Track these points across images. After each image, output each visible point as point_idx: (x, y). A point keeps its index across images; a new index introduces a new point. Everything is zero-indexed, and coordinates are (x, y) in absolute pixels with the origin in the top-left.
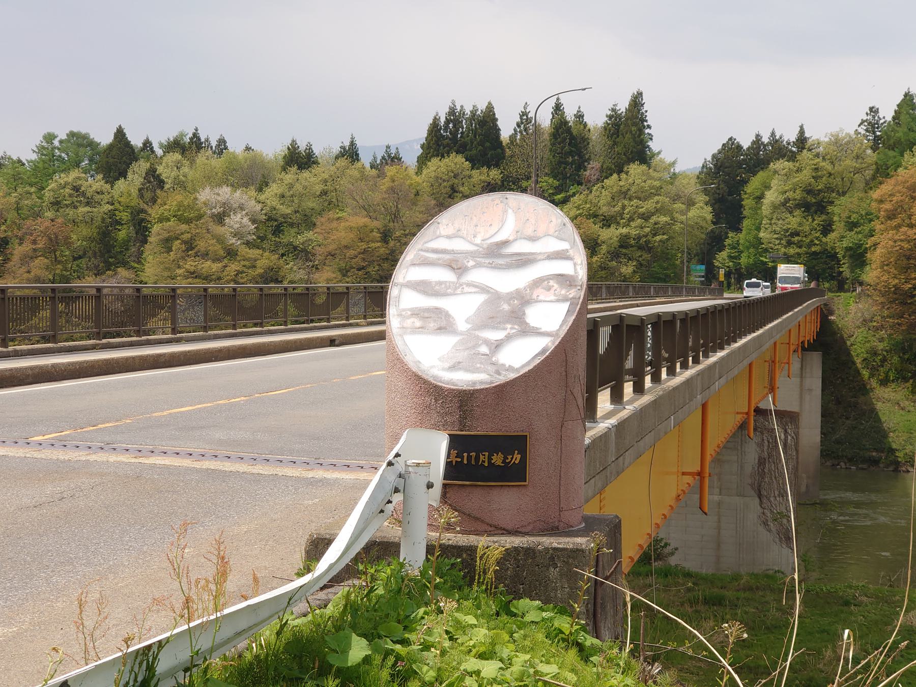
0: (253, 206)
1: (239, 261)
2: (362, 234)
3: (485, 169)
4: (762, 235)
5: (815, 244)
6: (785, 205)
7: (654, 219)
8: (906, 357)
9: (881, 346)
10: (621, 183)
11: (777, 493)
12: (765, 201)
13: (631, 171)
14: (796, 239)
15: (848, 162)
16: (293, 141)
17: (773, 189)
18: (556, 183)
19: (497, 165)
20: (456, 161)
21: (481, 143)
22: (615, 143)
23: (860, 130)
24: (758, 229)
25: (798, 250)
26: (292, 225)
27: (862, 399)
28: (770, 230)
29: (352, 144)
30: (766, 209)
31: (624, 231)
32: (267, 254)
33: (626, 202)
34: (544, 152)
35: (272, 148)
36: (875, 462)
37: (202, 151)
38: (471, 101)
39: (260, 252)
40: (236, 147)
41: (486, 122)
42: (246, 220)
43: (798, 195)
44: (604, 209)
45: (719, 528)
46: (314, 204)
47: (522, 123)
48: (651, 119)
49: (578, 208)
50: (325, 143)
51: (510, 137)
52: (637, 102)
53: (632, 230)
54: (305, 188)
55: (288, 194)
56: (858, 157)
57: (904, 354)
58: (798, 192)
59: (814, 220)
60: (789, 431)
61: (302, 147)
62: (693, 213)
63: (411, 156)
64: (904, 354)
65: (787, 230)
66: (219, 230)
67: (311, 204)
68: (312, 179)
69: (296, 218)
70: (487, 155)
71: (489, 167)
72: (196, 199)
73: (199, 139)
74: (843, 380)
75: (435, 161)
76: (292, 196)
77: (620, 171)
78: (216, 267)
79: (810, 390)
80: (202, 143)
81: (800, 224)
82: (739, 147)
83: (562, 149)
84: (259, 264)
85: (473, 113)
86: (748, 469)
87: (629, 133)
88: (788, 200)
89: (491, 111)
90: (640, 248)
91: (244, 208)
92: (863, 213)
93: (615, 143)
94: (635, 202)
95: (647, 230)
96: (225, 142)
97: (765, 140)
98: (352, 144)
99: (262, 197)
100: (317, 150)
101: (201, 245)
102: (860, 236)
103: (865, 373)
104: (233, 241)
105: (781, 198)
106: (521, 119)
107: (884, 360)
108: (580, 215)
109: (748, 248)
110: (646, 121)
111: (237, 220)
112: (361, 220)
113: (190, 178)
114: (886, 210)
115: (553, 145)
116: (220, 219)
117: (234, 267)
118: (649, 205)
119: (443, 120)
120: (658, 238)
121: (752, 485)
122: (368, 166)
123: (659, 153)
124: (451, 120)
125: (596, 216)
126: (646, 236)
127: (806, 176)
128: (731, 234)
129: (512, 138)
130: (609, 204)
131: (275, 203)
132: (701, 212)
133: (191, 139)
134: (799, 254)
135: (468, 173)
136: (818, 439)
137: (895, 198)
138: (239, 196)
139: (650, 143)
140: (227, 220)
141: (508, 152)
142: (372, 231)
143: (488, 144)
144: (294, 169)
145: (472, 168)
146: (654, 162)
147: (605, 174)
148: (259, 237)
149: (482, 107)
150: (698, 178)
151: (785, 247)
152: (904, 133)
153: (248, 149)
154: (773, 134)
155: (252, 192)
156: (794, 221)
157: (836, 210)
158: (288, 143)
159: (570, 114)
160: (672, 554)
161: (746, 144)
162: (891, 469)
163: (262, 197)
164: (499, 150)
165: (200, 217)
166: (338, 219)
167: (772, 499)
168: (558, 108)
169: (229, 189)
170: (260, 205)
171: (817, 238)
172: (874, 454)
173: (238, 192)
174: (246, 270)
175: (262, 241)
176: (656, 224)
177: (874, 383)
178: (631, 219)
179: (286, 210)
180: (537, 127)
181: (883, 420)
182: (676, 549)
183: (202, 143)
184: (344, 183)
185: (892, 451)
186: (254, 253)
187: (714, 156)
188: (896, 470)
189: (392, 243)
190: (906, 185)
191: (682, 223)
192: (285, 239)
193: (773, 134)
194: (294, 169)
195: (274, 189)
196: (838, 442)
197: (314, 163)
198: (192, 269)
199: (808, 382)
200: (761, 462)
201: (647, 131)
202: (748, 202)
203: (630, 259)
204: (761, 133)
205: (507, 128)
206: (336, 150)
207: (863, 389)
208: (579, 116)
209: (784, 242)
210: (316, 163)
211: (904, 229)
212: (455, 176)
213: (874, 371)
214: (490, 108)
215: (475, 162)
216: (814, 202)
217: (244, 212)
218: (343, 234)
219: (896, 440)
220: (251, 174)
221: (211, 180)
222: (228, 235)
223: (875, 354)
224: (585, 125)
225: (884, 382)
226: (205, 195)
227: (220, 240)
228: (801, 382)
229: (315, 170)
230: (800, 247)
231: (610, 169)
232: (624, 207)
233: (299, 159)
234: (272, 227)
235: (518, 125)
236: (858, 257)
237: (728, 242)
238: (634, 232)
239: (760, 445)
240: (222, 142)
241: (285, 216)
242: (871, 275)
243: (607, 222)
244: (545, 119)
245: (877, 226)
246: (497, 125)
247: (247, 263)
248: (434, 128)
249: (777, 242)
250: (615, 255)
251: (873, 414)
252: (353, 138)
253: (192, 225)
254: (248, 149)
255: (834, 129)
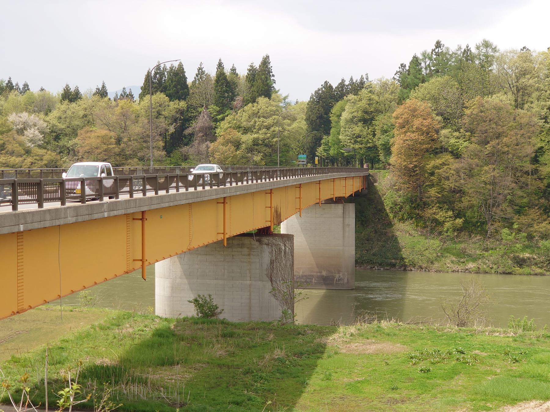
0: (42, 124)
1: (33, 156)
2: (105, 140)
3: (177, 101)
4: (340, 137)
5: (369, 143)
6: (351, 121)
7: (272, 129)
8: (413, 206)
9: (399, 200)
10: (254, 108)
11: (281, 279)
12: (342, 118)
13: (260, 102)
14: (359, 139)
15: (387, 96)
16: (67, 85)
17: (346, 111)
18: (218, 109)
19: (184, 99)
20: (160, 97)
21: (175, 86)
22: (252, 85)
23: (396, 77)
24: (339, 134)
25: (360, 146)
26: (66, 135)
27: (388, 230)
28: (344, 134)
29: (104, 87)
30: (342, 123)
31: (256, 136)
32: (49, 152)
33: (257, 119)
34: (211, 91)
35: (55, 91)
36: (394, 265)
37: (13, 91)
38: (169, 61)
39: (46, 151)
40: (34, 89)
41: (178, 74)
42: (37, 132)
43: (360, 114)
44: (245, 123)
45: (250, 299)
46: (79, 123)
47: (199, 74)
48: (274, 71)
49: (229, 123)
50: (87, 87)
51: (193, 82)
52: (265, 62)
53: (260, 136)
54: (73, 113)
55: (63, 117)
56: (392, 93)
57: (412, 204)
58: (360, 112)
59: (368, 129)
60: (287, 245)
61: (72, 89)
62: (295, 125)
63: (136, 94)
64: (412, 204)
65: (354, 134)
66: (21, 138)
67: (76, 122)
68: (77, 108)
69: (68, 131)
70: (178, 93)
71: (179, 100)
72: (7, 120)
73: (12, 84)
74: (379, 220)
75: (148, 97)
76: (65, 118)
77: (254, 101)
78: (18, 160)
79: (349, 225)
80: (13, 87)
81: (361, 131)
82: (331, 87)
83: (222, 89)
84: (45, 158)
85: (171, 68)
86: (265, 266)
87: (261, 80)
88: (354, 117)
89: (181, 67)
90: (266, 145)
91: (36, 125)
92: (389, 125)
93: (252, 85)
94: (262, 119)
95: (268, 135)
96: (28, 86)
97: (347, 83)
98: (104, 87)
99: (47, 119)
100: (82, 91)
101: (9, 147)
102: (388, 138)
103: (391, 215)
104: (29, 144)
105: (351, 116)
106: (199, 72)
107: (401, 208)
108: (230, 127)
109: (334, 145)
110: (272, 72)
111: (31, 133)
112: (104, 132)
113: (4, 107)
114: (399, 123)
115: (216, 87)
116: (21, 132)
117: (29, 160)
118: (269, 121)
119: (153, 73)
120: (275, 140)
121: (267, 275)
122: (112, 99)
123: (279, 91)
124: (158, 73)
125: (239, 127)
126: (268, 139)
127: (363, 104)
128: (325, 137)
129: (194, 82)
130: (247, 121)
131: (55, 122)
132: (301, 125)
133: (7, 84)
134: (360, 148)
135: (167, 103)
136: (354, 252)
137: (404, 116)
138: (33, 118)
139: (274, 85)
140: (26, 132)
141: (191, 91)
142: (111, 138)
143: (179, 87)
144: (66, 102)
145: (170, 101)
146: (273, 96)
147: (245, 103)
148: (45, 142)
149: (176, 65)
150: (308, 104)
151: (353, 144)
152: (412, 79)
153: (42, 90)
154: (351, 79)
155: (42, 115)
156: (358, 129)
157: (377, 123)
158: (64, 86)
159: (227, 70)
160: (221, 313)
161: (335, 85)
162: (402, 269)
163: (47, 119)
164: (186, 90)
165: (10, 130)
166: (92, 131)
167: (278, 282)
168: (220, 65)
169: (27, 114)
170: (46, 123)
171: (370, 139)
172: (393, 261)
173: (33, 115)
174: (36, 162)
175: (48, 144)
176: (273, 131)
177: (396, 220)
178: (260, 129)
179: (62, 126)
180: (208, 76)
181: (400, 241)
182: (223, 310)
183: (13, 87)
184: (97, 110)
185: (403, 259)
186: (42, 151)
187: (316, 92)
188: (405, 270)
189: (122, 145)
190: (410, 108)
191: (289, 131)
192: (61, 143)
193: (351, 79)
194: (66, 102)
195: (55, 114)
196: (374, 255)
197: (80, 98)
198: (4, 161)
199: (347, 221)
200: (272, 262)
201: (272, 78)
202: (333, 118)
203: (259, 152)
204: (345, 79)
205: (190, 77)
206: (94, 91)
207: (390, 225)
208: (233, 70)
209: (352, 141)
210: (80, 98)
211: (409, 134)
212: (160, 106)
213: (396, 214)
214: (181, 66)
215: (171, 97)
216: (367, 119)
217: (36, 128)
218: (93, 140)
219: (405, 253)
220: (43, 105)
221: (18, 109)
222: (26, 142)
223: (396, 205)
224: (237, 75)
225: (402, 220)
226: (12, 117)
227: (21, 144)
228: (344, 220)
229: (80, 102)
230: (362, 144)
231: (248, 100)
232: (255, 122)
233: (71, 96)
234: (54, 136)
235: (197, 76)
236: (387, 150)
237: (323, 141)
238: (261, 137)
239: (271, 253)
240: (26, 86)
241: (61, 130)
242: (392, 160)
243: (246, 131)
244: (212, 72)
245: (396, 132)
246: (185, 76)
247: (37, 158)
248: (148, 76)
249: (349, 141)
250: (250, 150)
251: (394, 239)
252: (104, 83)
253: (4, 135)
254: (42, 90)
255: (379, 77)
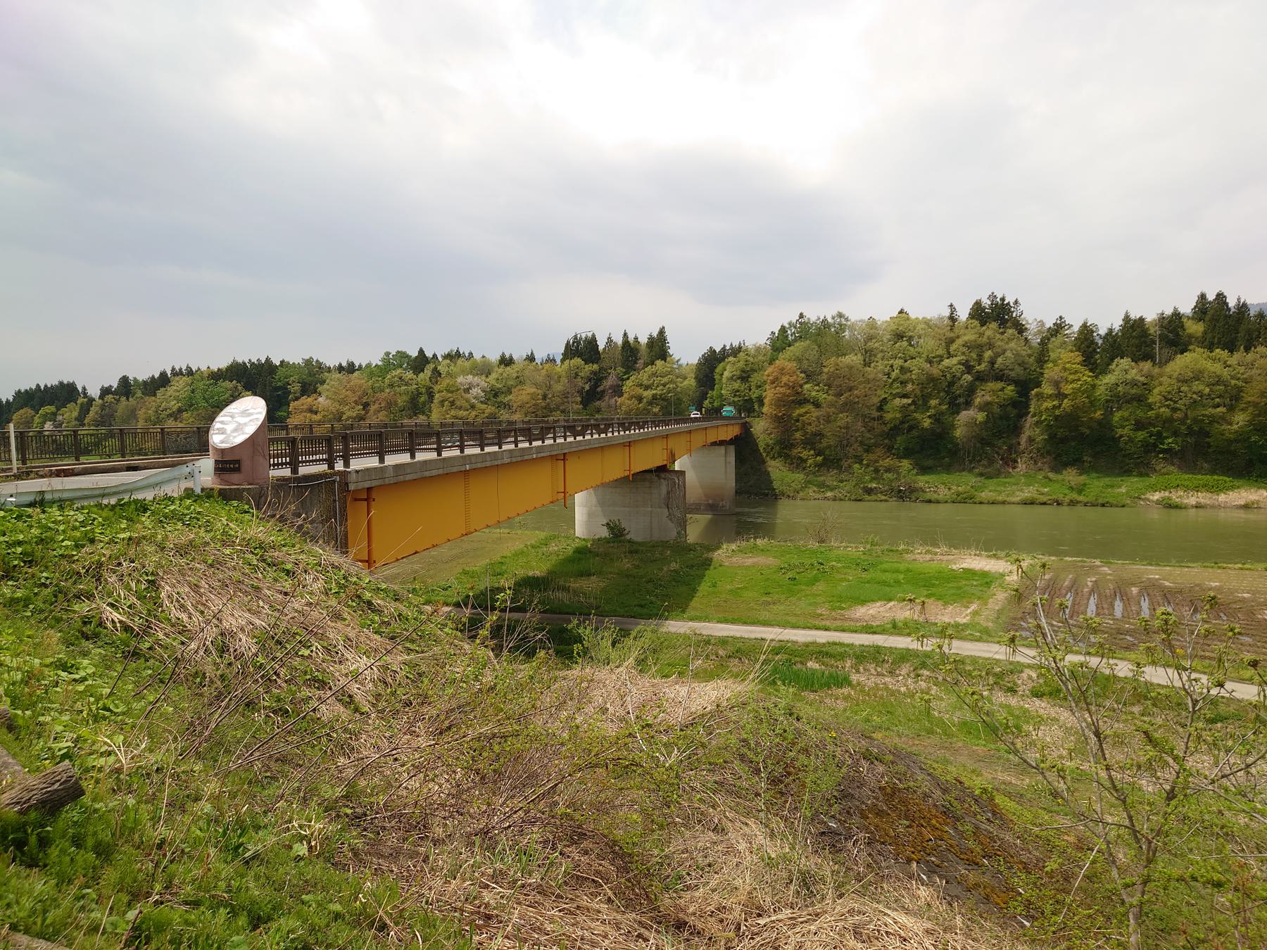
0: (484, 384)
17: (727, 371)
20: (578, 361)
30: (724, 380)
35: (494, 357)
38: (584, 331)
40: (477, 356)
41: (592, 342)
43: (738, 373)
50: (519, 354)
52: (662, 332)
62: (686, 383)
63: (558, 359)
87: (658, 346)
91: (479, 385)
100: (515, 357)
101: (458, 403)
111: (475, 391)
116: (467, 391)
117: (474, 413)
118: (665, 380)
127: (741, 364)
131: (494, 382)
132: (691, 382)
149: (590, 335)
156: (736, 385)
159: (631, 338)
168: (625, 334)
184: (527, 373)
186: (484, 406)
195: (494, 376)
200: (668, 493)
202: (717, 377)
205: (601, 345)
207: (764, 462)
208: (636, 338)
213: (768, 453)
214: (594, 335)
216: (744, 376)
219: (776, 485)
220: (484, 369)
221: (464, 372)
225: (773, 458)
226: (460, 379)
233: (506, 361)
234: (493, 394)
236: (761, 401)
240: (471, 354)
242: (765, 410)
243: (647, 388)
244: (619, 340)
245: (767, 387)
250: (650, 403)
